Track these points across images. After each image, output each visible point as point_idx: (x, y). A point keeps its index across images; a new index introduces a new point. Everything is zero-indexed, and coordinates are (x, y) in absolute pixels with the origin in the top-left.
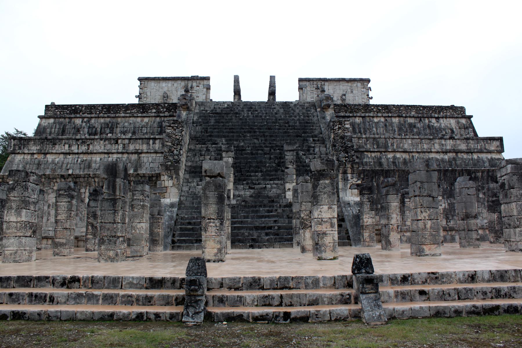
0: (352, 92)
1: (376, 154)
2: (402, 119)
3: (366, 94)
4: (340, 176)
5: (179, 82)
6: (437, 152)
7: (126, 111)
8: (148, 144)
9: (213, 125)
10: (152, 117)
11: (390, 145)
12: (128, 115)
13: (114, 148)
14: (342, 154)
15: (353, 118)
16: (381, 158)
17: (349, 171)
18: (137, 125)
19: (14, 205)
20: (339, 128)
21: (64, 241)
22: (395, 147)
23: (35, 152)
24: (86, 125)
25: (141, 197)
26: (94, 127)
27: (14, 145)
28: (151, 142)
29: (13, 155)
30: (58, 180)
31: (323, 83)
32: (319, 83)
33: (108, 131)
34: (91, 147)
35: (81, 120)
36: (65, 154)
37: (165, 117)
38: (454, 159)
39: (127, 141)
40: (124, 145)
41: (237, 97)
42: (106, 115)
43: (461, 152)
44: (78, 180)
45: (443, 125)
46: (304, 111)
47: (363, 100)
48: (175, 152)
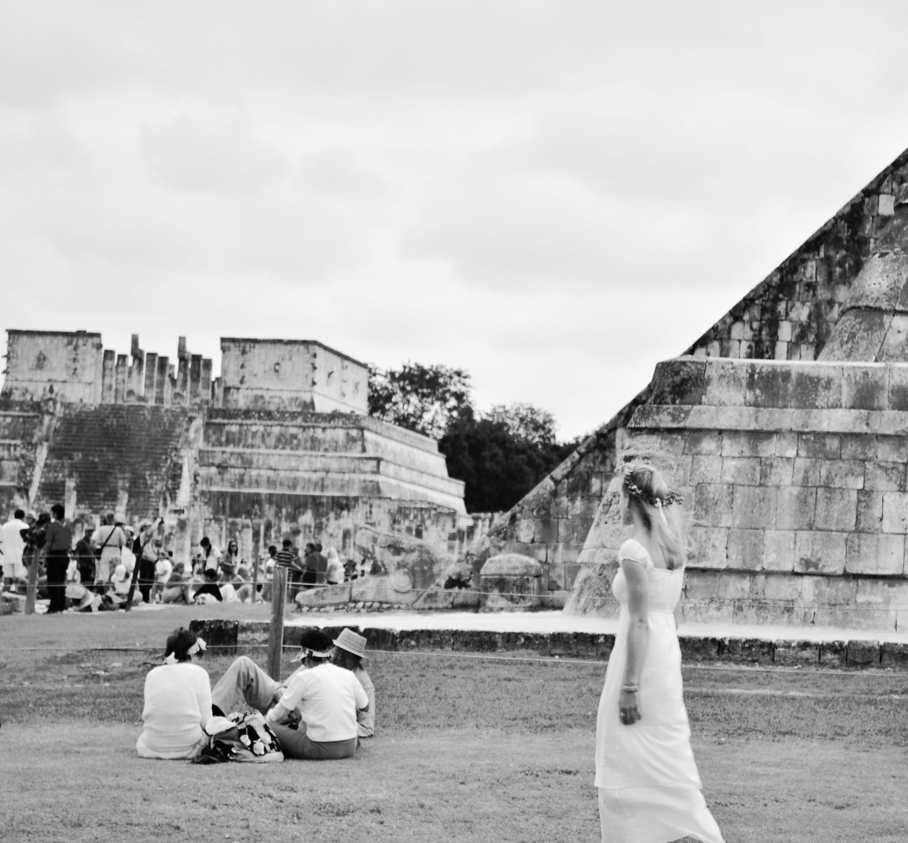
0: (290, 359)
2: (283, 428)
4: (161, 502)
5: (60, 338)
6: (306, 471)
8: (9, 450)
14: (170, 482)
16: (244, 475)
28: (12, 449)
32: (248, 346)
45: (328, 438)
46: (172, 419)
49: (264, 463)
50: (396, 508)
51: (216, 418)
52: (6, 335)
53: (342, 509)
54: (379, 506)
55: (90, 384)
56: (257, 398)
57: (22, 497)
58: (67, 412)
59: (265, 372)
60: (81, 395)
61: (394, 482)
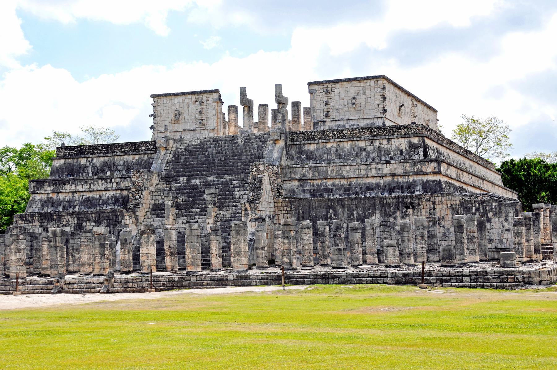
1: (318, 181)
3: (380, 94)
5: (190, 96)
7: (121, 149)
9: (182, 165)
10: (141, 154)
11: (330, 172)
12: (122, 154)
13: (109, 186)
15: (309, 145)
17: (249, 208)
18: (130, 162)
19: (13, 251)
20: (256, 170)
21: (47, 266)
22: (334, 174)
23: (49, 192)
25: (85, 240)
29: (34, 195)
30: (66, 217)
31: (333, 86)
34: (92, 186)
35: (85, 159)
36: (73, 192)
37: (151, 154)
38: (389, 184)
39: (119, 180)
40: (117, 183)
41: (246, 109)
43: (398, 176)
45: (393, 147)
47: (376, 102)
48: (137, 197)
49: (337, 174)
51: (297, 141)
52: (151, 100)
53: (408, 208)
55: (213, 129)
57: (131, 217)
58: (179, 146)
59: (345, 106)
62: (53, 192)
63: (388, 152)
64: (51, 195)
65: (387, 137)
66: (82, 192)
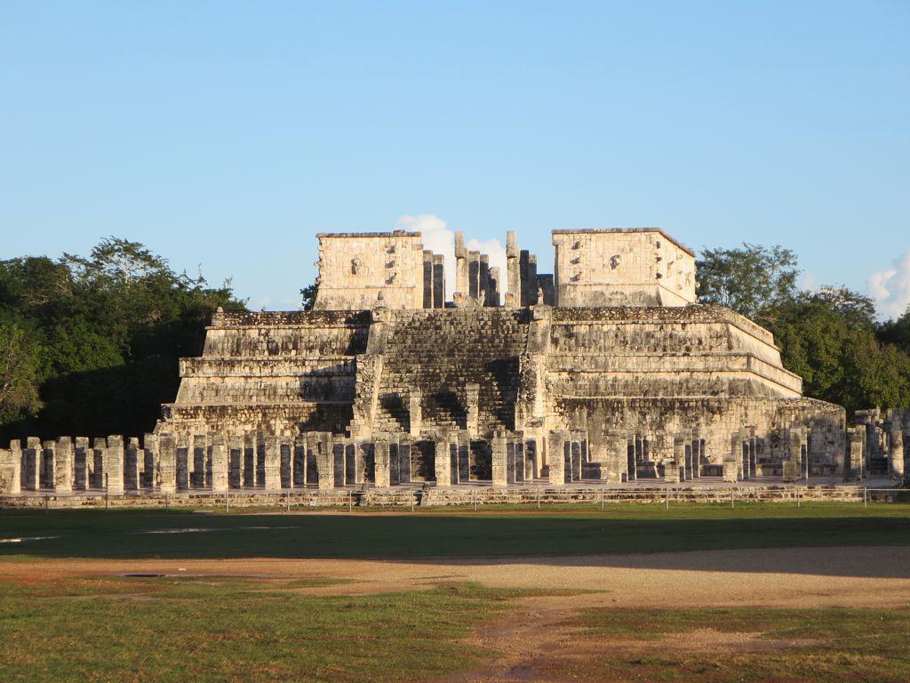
1: (594, 374)
16: (598, 380)
17: (524, 410)
24: (264, 338)
26: (274, 341)
27: (187, 367)
30: (246, 411)
33: (291, 346)
34: (275, 369)
36: (246, 377)
38: (687, 381)
42: (287, 327)
44: (267, 411)
50: (775, 408)
53: (714, 413)
54: (756, 408)
56: (596, 295)
60: (404, 302)
61: (759, 379)
62: (216, 375)
63: (683, 341)
64: (212, 380)
65: (682, 322)
66: (260, 377)
